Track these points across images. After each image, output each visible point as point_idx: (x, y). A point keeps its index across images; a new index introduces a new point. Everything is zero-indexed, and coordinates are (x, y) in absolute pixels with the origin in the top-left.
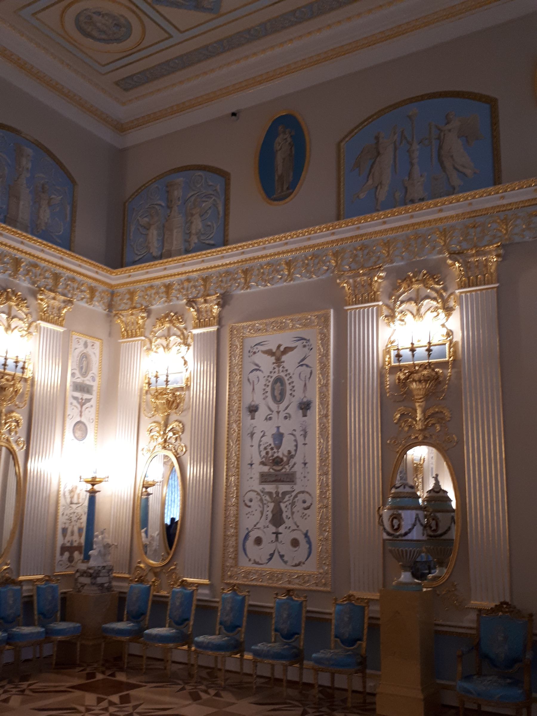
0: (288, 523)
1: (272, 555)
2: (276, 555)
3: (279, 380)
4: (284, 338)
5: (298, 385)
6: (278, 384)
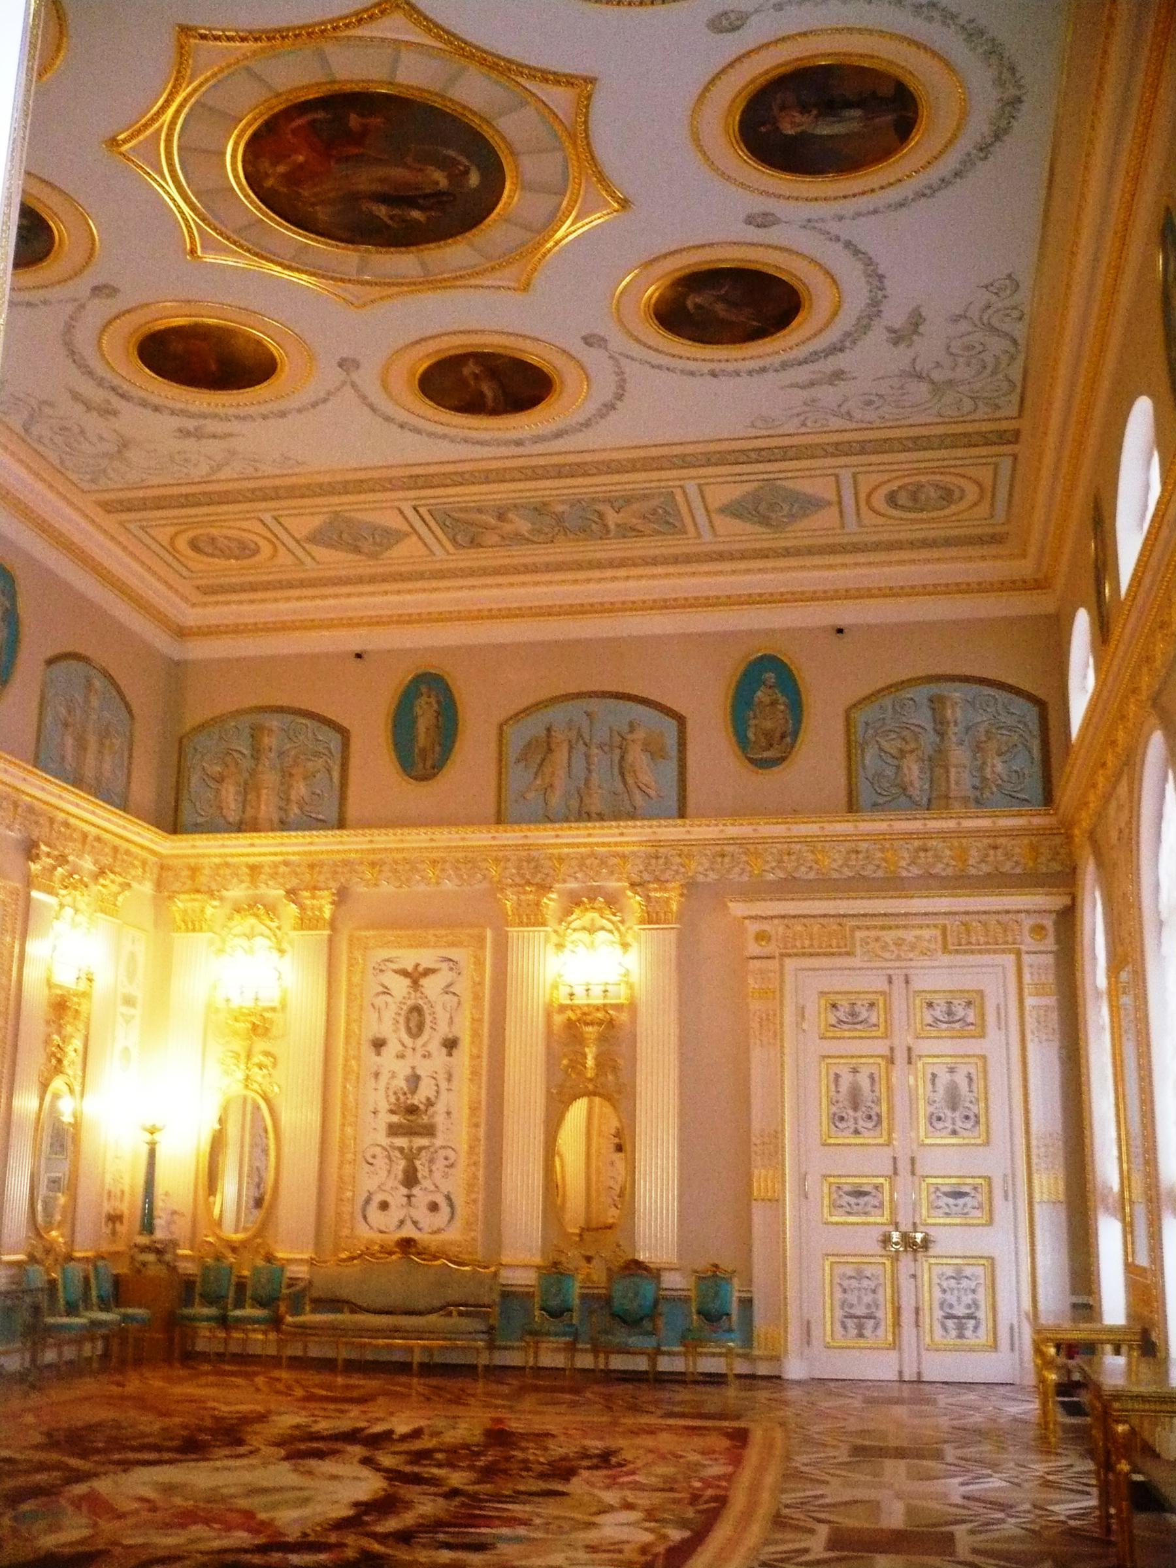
0: (426, 1183)
1: (402, 1222)
2: (409, 1222)
3: (417, 1009)
4: (425, 957)
5: (443, 1018)
6: (415, 1014)
